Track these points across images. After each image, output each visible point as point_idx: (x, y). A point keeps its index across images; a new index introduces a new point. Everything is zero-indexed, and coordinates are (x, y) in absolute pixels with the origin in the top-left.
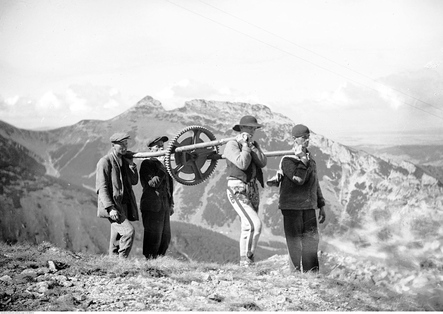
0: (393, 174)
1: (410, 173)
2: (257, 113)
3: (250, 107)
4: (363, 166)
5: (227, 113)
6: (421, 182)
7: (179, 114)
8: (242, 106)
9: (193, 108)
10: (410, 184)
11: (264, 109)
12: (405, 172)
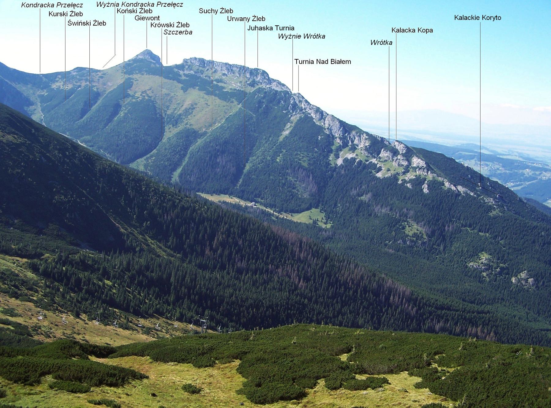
0: (384, 154)
1: (401, 153)
4: (355, 143)
5: (224, 74)
6: (410, 163)
8: (240, 68)
10: (399, 165)
12: (395, 152)
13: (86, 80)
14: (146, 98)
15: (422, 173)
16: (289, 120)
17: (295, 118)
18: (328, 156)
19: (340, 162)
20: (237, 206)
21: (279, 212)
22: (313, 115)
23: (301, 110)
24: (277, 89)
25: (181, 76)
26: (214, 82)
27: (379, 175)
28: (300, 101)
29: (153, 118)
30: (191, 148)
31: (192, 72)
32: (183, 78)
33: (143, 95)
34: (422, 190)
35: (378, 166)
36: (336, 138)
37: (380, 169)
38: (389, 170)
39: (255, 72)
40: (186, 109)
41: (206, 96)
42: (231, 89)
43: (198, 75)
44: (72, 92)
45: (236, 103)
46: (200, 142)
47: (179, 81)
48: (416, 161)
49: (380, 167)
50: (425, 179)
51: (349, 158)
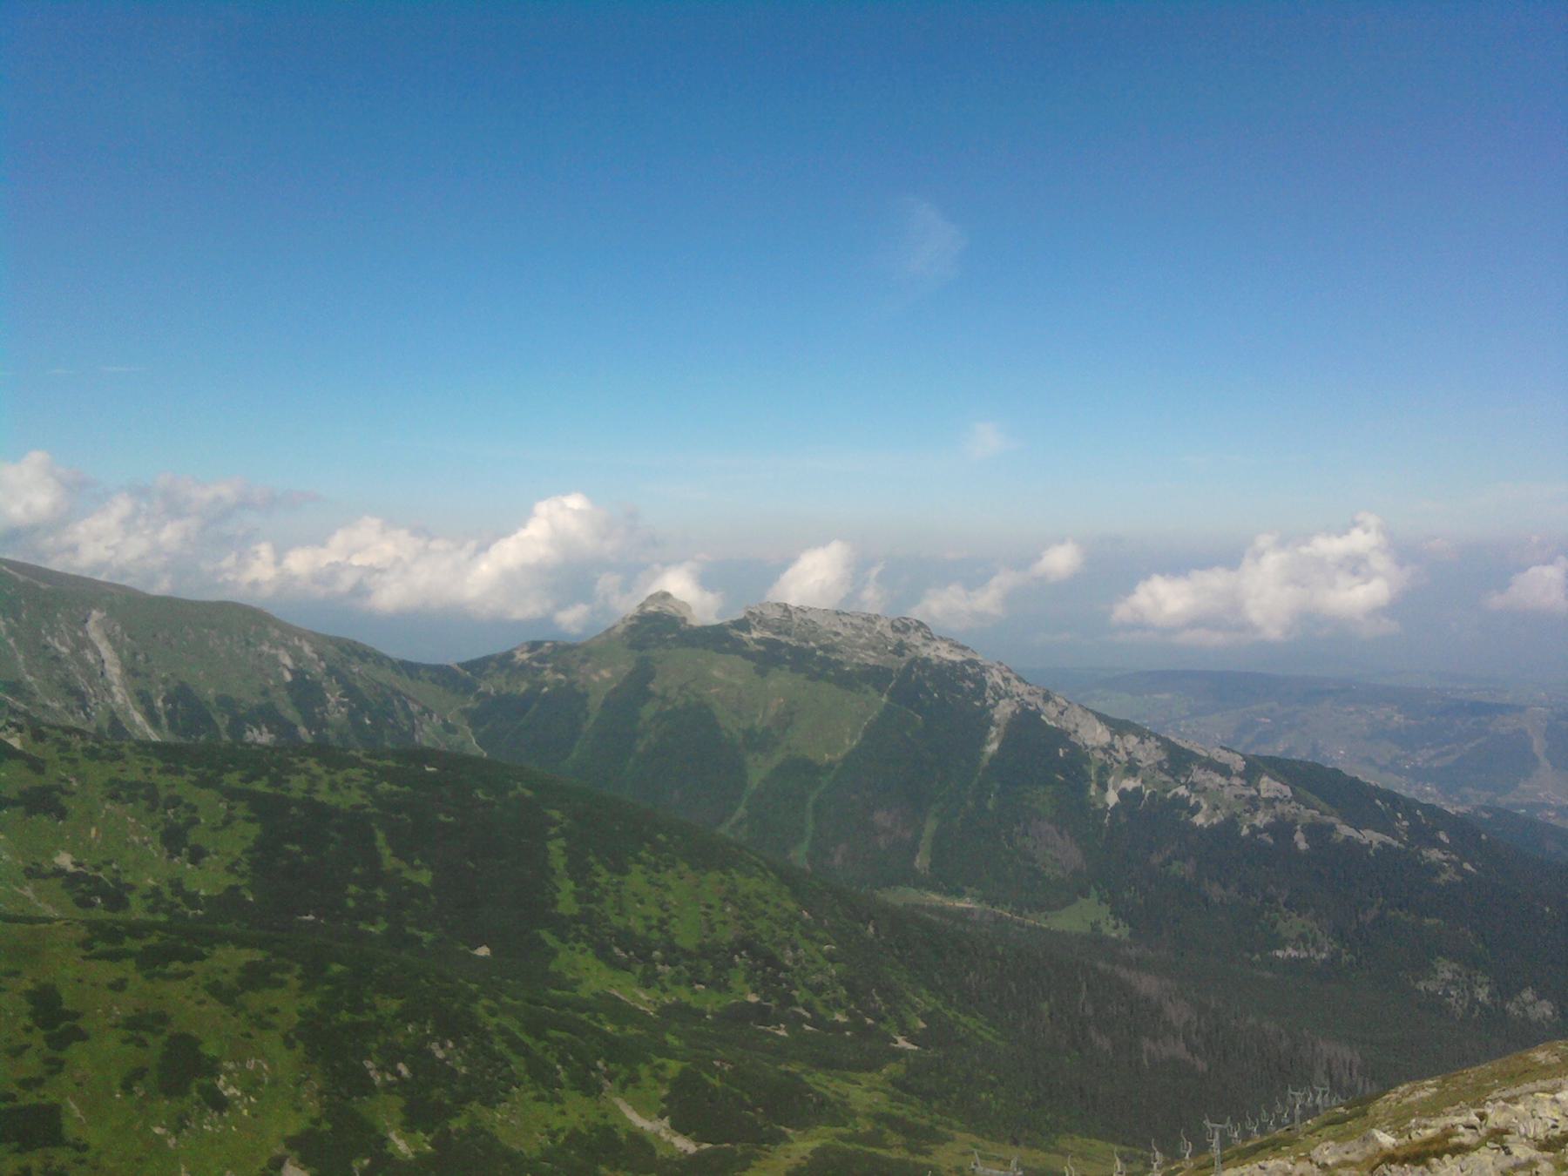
2: (903, 637)
3: (887, 623)
7: (734, 632)
9: (763, 623)
11: (917, 629)
12: (1224, 770)
13: (555, 670)
15: (1289, 809)
16: (991, 721)
17: (1004, 710)
18: (1085, 790)
19: (1112, 798)
25: (746, 644)
26: (819, 653)
27: (1199, 820)
31: (768, 634)
32: (753, 647)
34: (1296, 845)
35: (1192, 802)
37: (1195, 810)
38: (1216, 808)
42: (858, 665)
43: (783, 639)
45: (873, 693)
47: (749, 656)
48: (1268, 786)
49: (1198, 803)
50: (1294, 822)
51: (1130, 789)
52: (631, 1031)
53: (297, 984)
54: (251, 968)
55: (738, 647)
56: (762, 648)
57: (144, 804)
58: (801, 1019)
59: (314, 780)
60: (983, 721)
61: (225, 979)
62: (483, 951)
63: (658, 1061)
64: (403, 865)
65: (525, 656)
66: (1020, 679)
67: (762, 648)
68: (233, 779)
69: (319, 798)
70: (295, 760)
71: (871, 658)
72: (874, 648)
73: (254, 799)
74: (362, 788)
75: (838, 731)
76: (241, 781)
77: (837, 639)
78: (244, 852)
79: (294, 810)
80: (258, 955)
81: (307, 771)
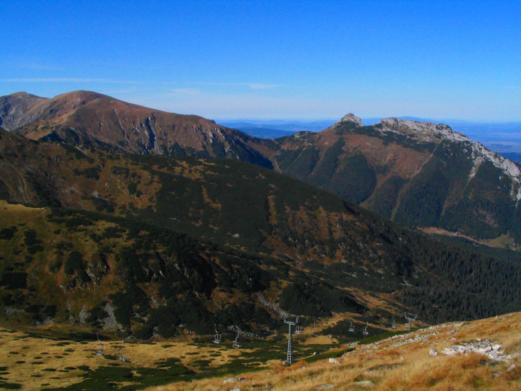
2: (441, 131)
3: (435, 126)
5: (415, 130)
7: (376, 129)
8: (427, 124)
9: (387, 125)
11: (446, 128)
13: (308, 142)
14: (358, 153)
16: (473, 165)
17: (478, 161)
18: (508, 192)
20: (445, 236)
21: (478, 239)
22: (492, 160)
23: (482, 156)
24: (459, 140)
25: (380, 133)
28: (480, 149)
29: (365, 170)
30: (400, 192)
31: (389, 130)
32: (383, 134)
33: (355, 151)
36: (513, 177)
39: (440, 127)
40: (390, 160)
41: (404, 149)
42: (422, 142)
43: (394, 131)
44: (299, 151)
46: (406, 187)
47: (380, 137)
52: (272, 268)
53: (125, 237)
54: (109, 230)
55: (377, 135)
56: (386, 135)
57: (124, 175)
58: (363, 271)
59: (184, 169)
60: (469, 164)
61: (98, 233)
62: (237, 235)
63: (280, 281)
64: (211, 201)
65: (298, 137)
66: (485, 149)
67: (386, 135)
68: (155, 167)
69: (184, 175)
70: (178, 162)
71: (428, 139)
72: (429, 136)
73: (161, 175)
74: (200, 172)
75: (412, 167)
76: (158, 168)
77: (415, 132)
78: (155, 194)
79: (175, 179)
80: (113, 225)
81: (182, 166)
